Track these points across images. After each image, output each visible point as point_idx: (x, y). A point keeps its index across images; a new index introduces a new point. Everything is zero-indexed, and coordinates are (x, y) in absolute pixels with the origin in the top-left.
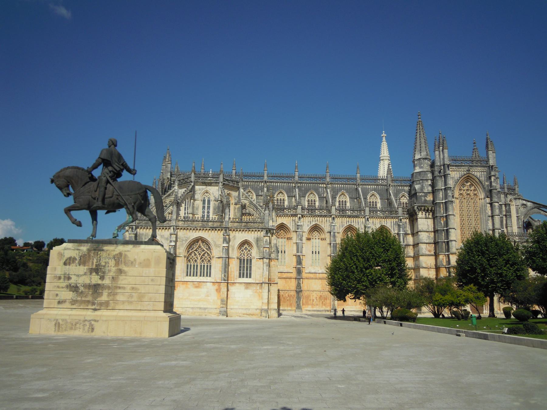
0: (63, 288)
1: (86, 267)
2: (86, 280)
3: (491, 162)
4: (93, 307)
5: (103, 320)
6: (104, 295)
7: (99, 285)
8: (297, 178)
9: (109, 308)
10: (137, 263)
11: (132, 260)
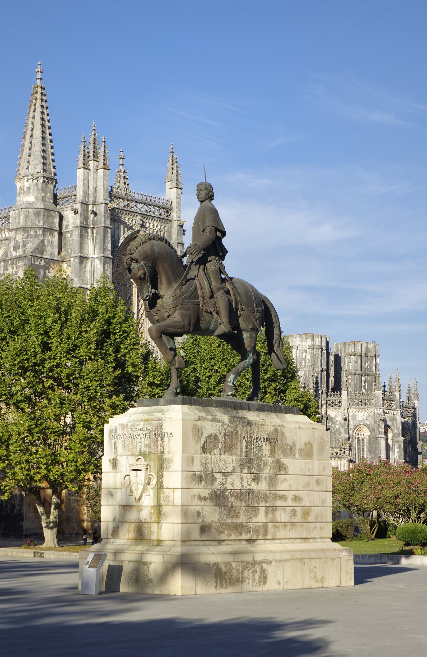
0: (205, 499)
1: (234, 457)
2: (235, 483)
4: (248, 537)
5: (276, 561)
6: (260, 511)
7: (252, 491)
9: (268, 538)
10: (297, 450)
11: (291, 444)
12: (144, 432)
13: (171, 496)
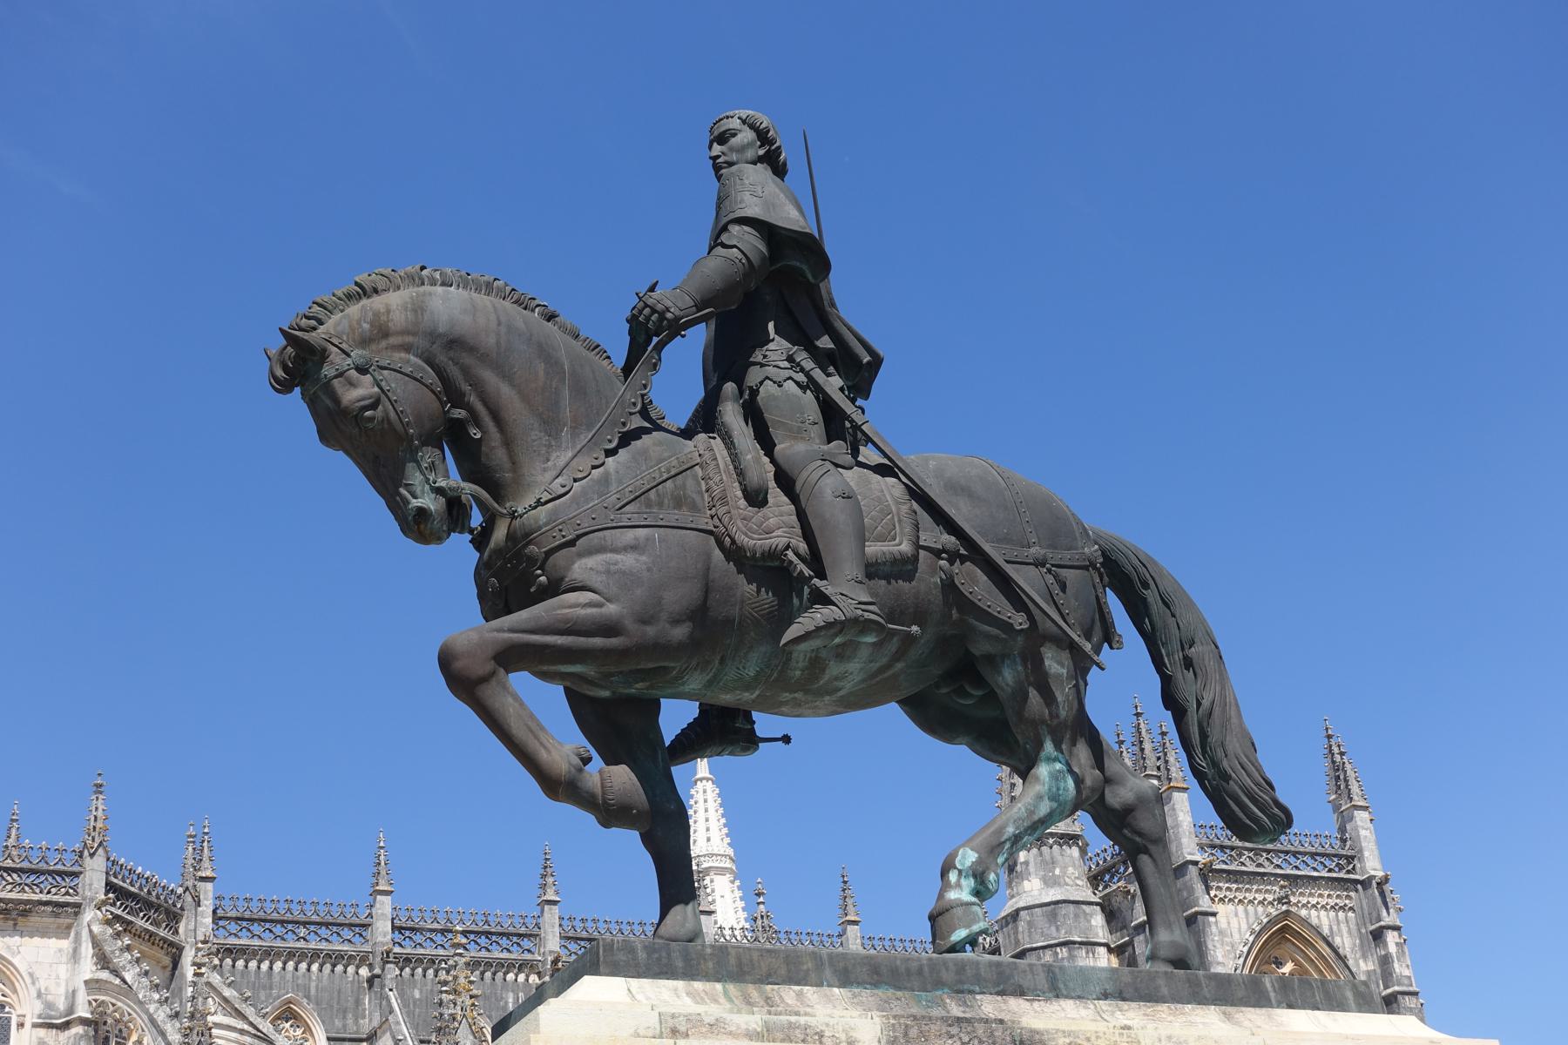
3: (1372, 865)
8: (382, 931)
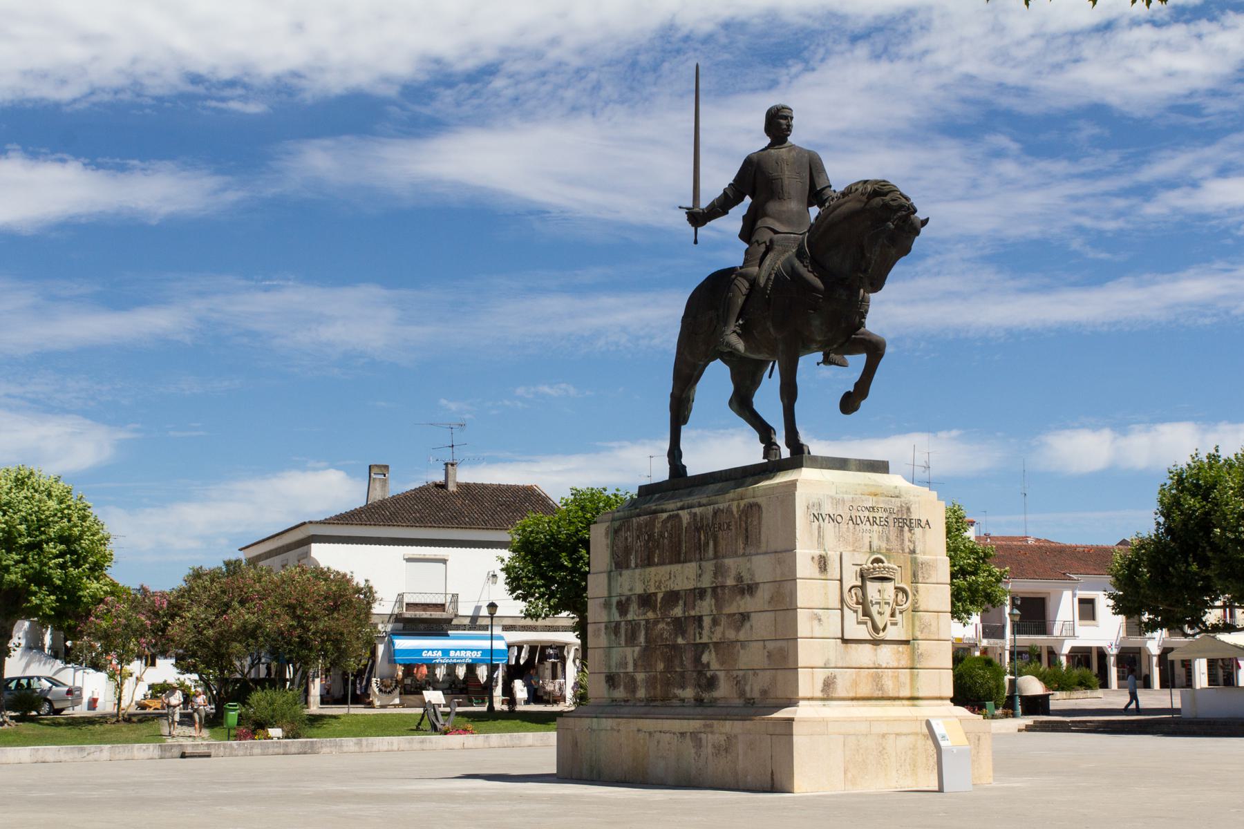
12: (877, 515)
13: (934, 624)
